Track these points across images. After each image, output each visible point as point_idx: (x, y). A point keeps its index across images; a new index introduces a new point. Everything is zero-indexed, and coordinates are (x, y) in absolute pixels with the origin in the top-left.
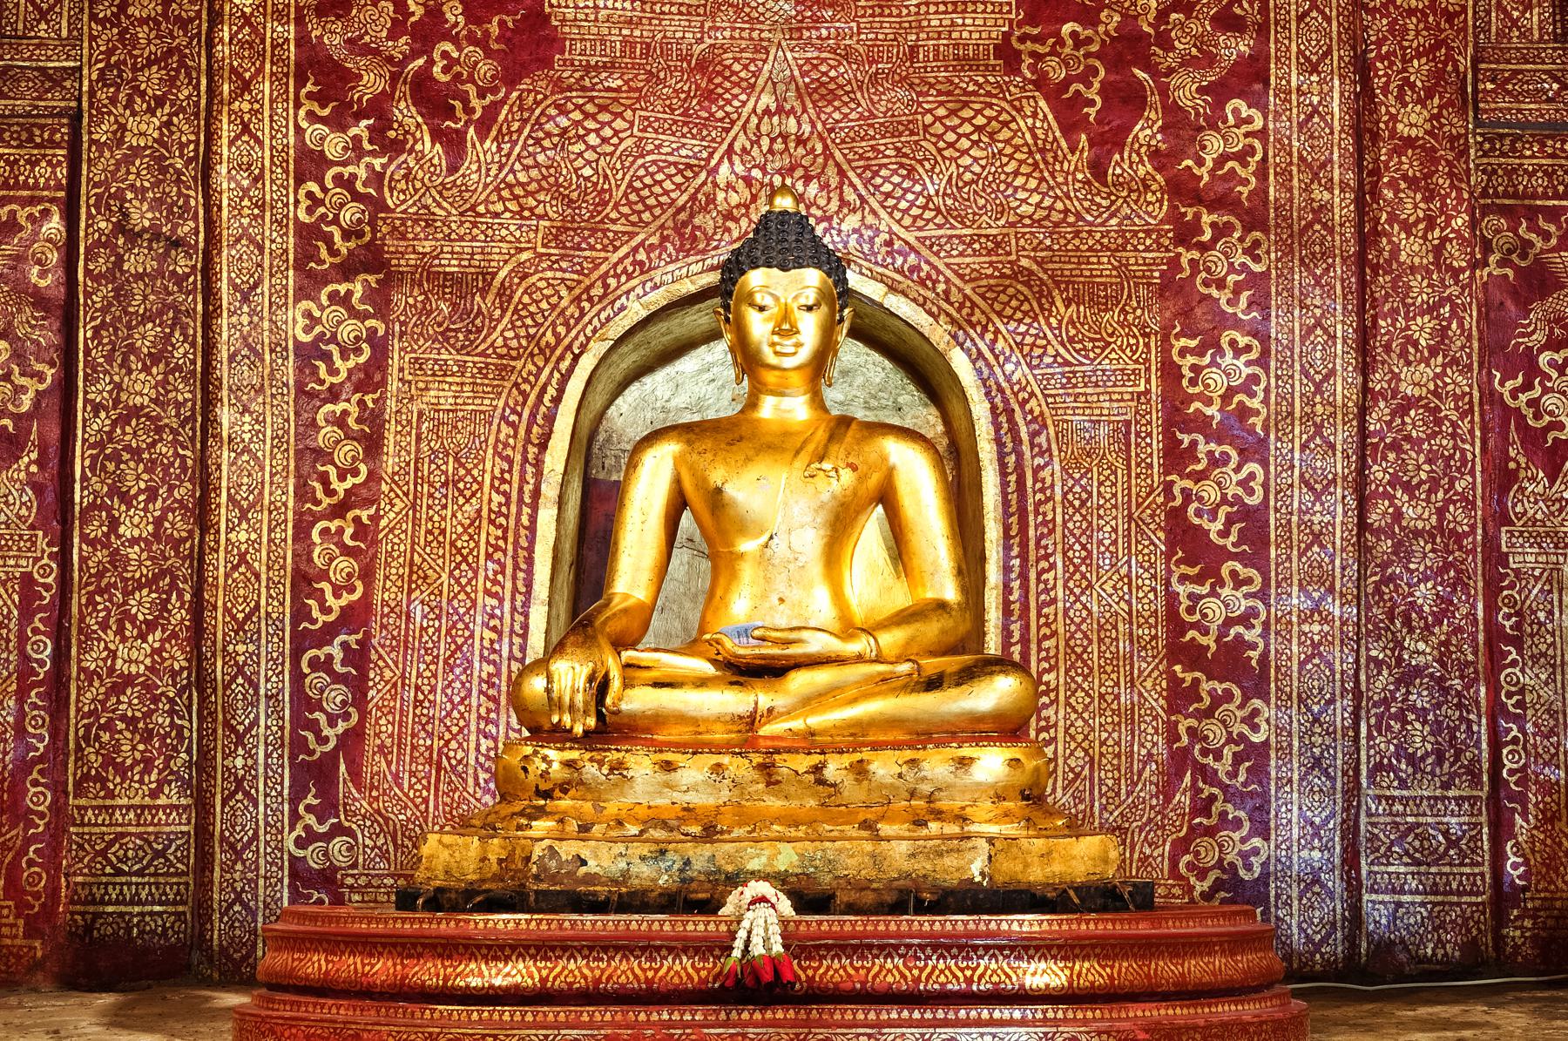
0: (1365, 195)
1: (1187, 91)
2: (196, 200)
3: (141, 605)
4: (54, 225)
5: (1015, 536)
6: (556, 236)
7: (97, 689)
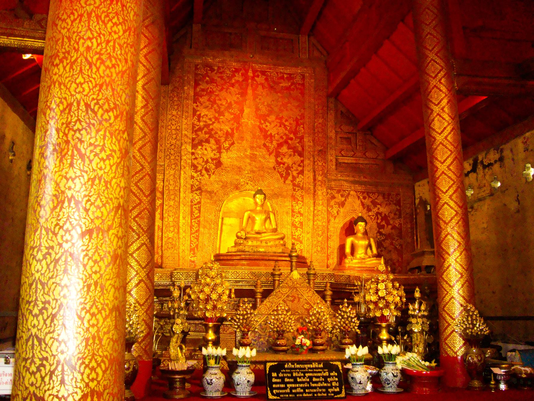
0: (315, 186)
1: (295, 173)
2: (178, 181)
4: (162, 183)
6: (222, 187)
7: (167, 239)
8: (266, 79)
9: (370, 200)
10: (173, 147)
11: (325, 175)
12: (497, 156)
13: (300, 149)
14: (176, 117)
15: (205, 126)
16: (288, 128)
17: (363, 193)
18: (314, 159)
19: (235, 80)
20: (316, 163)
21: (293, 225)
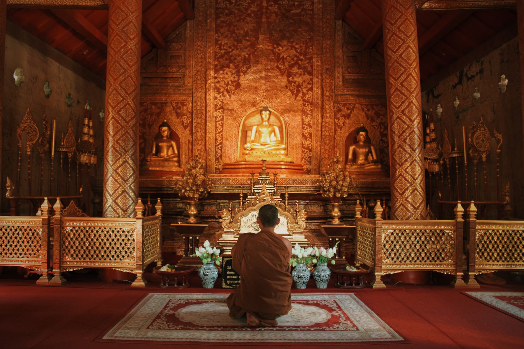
0: (323, 101)
1: (305, 91)
2: (204, 101)
3: (200, 142)
4: (191, 104)
5: (287, 136)
6: (241, 105)
8: (279, 8)
9: (374, 111)
10: (199, 73)
11: (332, 91)
12: (479, 68)
13: (309, 69)
14: (201, 47)
15: (225, 53)
16: (299, 50)
17: (367, 105)
18: (322, 76)
19: (251, 11)
20: (324, 81)
21: (303, 136)
